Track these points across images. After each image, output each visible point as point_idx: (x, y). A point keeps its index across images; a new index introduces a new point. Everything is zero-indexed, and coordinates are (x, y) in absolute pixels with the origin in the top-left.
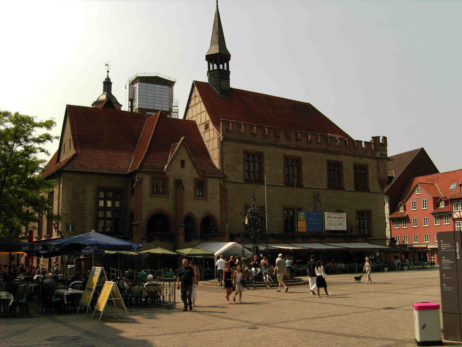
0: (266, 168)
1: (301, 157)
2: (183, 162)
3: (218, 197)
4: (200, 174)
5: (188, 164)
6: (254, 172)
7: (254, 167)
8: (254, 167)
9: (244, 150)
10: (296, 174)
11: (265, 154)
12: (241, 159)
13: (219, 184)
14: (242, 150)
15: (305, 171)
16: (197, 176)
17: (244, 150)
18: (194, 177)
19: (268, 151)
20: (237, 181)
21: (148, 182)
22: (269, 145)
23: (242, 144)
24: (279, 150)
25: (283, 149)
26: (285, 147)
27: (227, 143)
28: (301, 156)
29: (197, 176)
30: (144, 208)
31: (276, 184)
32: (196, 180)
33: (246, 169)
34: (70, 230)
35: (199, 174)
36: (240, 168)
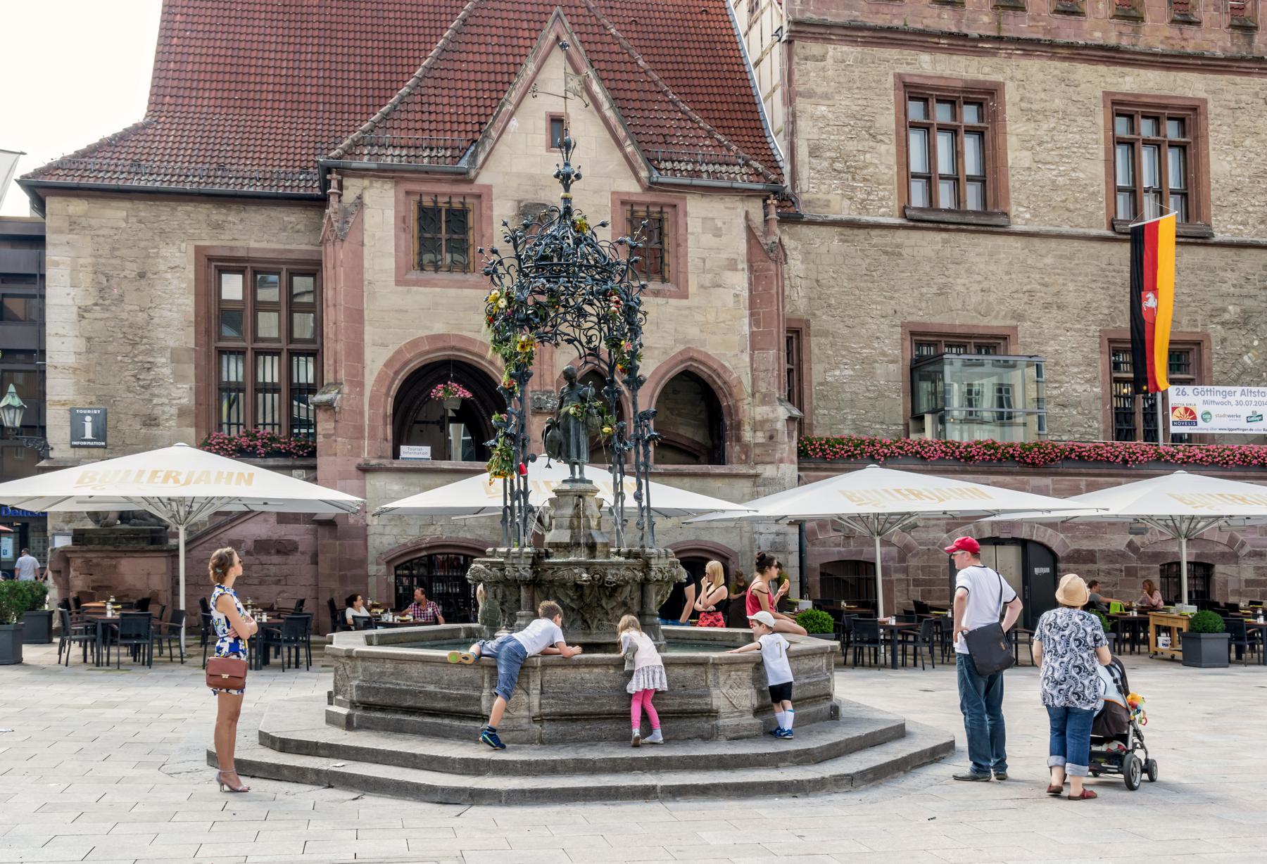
0: (1016, 156)
1: (1205, 101)
2: (557, 122)
3: (739, 281)
4: (644, 174)
5: (587, 131)
6: (955, 179)
7: (957, 155)
8: (957, 155)
9: (899, 77)
10: (1173, 182)
11: (1011, 94)
12: (888, 120)
13: (741, 222)
14: (891, 79)
15: (1222, 163)
16: (630, 186)
17: (899, 77)
18: (613, 193)
19: (1025, 83)
20: (865, 218)
21: (390, 215)
22: (1029, 46)
23: (893, 53)
24: (1082, 71)
25: (1102, 68)
26: (1110, 55)
27: (815, 48)
28: (1202, 95)
29: (630, 186)
30: (369, 333)
31: (1066, 229)
32: (626, 202)
33: (917, 165)
34: (88, 435)
35: (639, 180)
36: (883, 160)
